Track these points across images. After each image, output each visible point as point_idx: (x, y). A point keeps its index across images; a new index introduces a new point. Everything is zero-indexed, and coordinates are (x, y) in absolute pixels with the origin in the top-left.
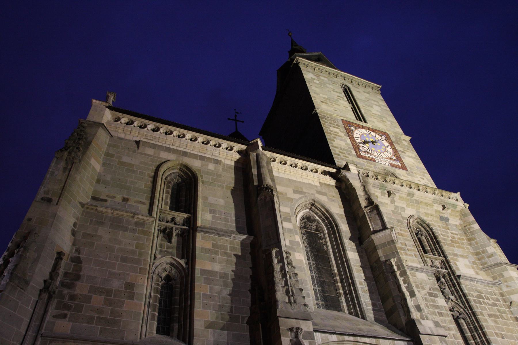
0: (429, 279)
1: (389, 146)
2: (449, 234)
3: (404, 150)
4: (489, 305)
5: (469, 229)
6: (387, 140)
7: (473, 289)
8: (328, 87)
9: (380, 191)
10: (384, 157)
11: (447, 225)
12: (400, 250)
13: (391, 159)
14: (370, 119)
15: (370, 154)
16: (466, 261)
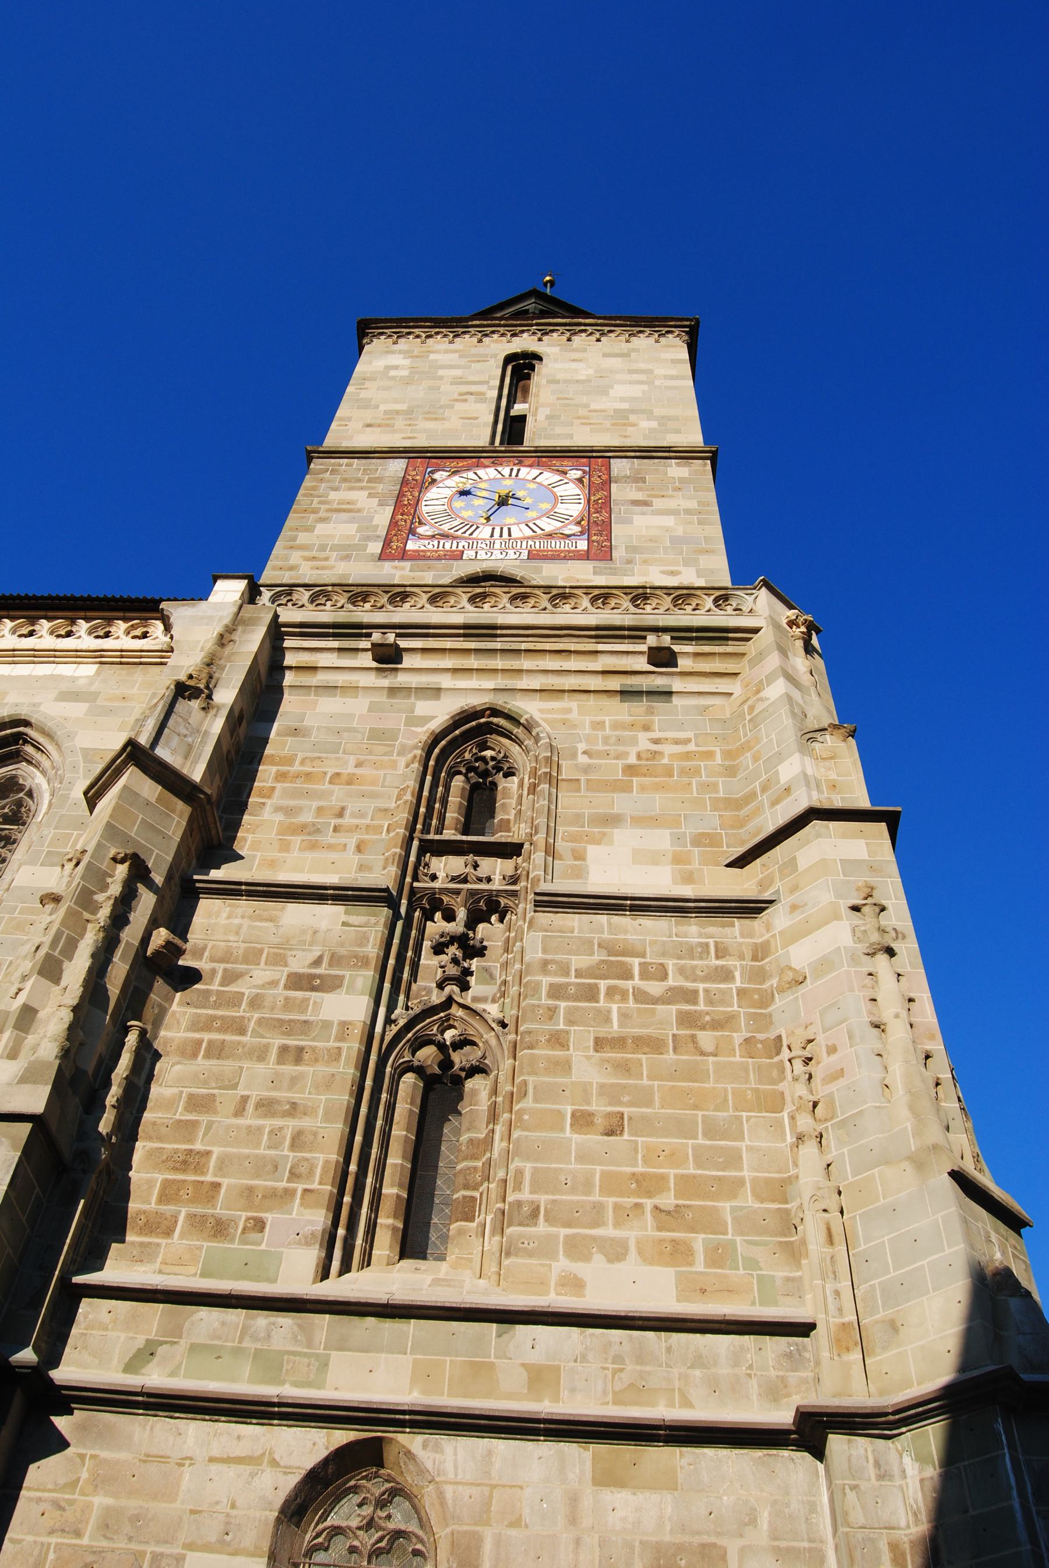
0: (344, 924)
1: (582, 497)
2: (634, 741)
3: (648, 496)
4: (641, 996)
5: (752, 708)
6: (586, 481)
7: (590, 942)
8: (441, 378)
9: (336, 644)
10: (521, 535)
11: (652, 713)
12: (291, 835)
13: (551, 535)
14: (558, 430)
15: (455, 538)
16: (661, 839)
